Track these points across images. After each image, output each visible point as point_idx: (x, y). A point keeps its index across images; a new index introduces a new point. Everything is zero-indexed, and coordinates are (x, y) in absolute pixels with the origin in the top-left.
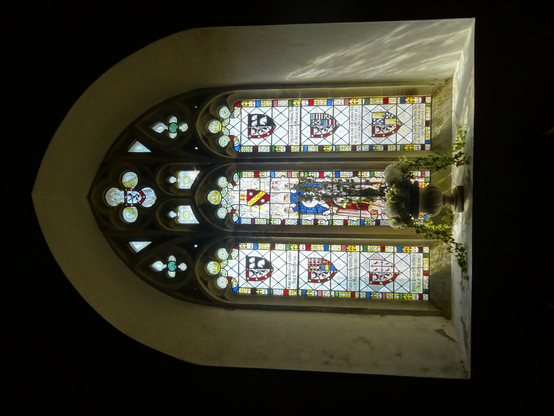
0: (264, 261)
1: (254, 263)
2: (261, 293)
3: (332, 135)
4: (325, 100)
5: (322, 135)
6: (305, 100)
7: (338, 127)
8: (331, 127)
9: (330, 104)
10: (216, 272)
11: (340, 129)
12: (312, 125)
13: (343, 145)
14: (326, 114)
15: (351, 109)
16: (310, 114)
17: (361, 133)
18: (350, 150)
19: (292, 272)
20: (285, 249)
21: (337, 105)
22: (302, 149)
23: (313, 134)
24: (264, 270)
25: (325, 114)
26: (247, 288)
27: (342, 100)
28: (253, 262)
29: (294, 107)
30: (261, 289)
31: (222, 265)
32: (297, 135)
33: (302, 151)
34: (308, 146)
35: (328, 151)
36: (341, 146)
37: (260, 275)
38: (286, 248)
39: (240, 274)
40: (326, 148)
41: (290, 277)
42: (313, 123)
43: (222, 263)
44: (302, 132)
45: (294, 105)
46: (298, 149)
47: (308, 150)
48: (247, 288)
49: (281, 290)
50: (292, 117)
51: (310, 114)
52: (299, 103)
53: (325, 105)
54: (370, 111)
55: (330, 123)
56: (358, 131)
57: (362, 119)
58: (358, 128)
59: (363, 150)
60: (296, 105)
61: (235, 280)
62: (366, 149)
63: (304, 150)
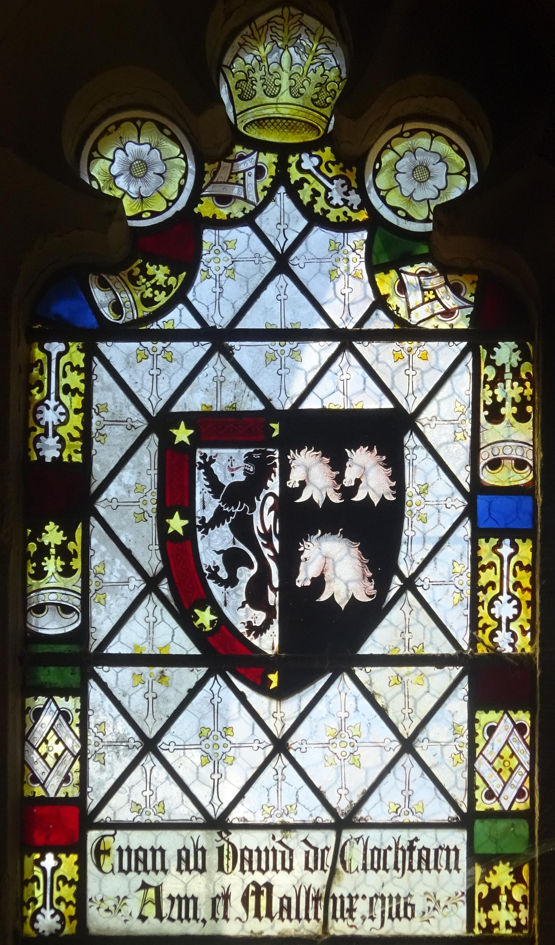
0: (362, 597)
1: (336, 499)
2: (40, 574)
10: (241, 105)
19: (261, 879)
20: (482, 805)
24: (273, 598)
26: (87, 422)
28: (348, 481)
30: (76, 564)
31: (309, 163)
37: (219, 560)
38: (490, 814)
39: (228, 354)
41: (212, 858)
43: (335, 170)
48: (87, 422)
49: (75, 777)
61: (162, 298)
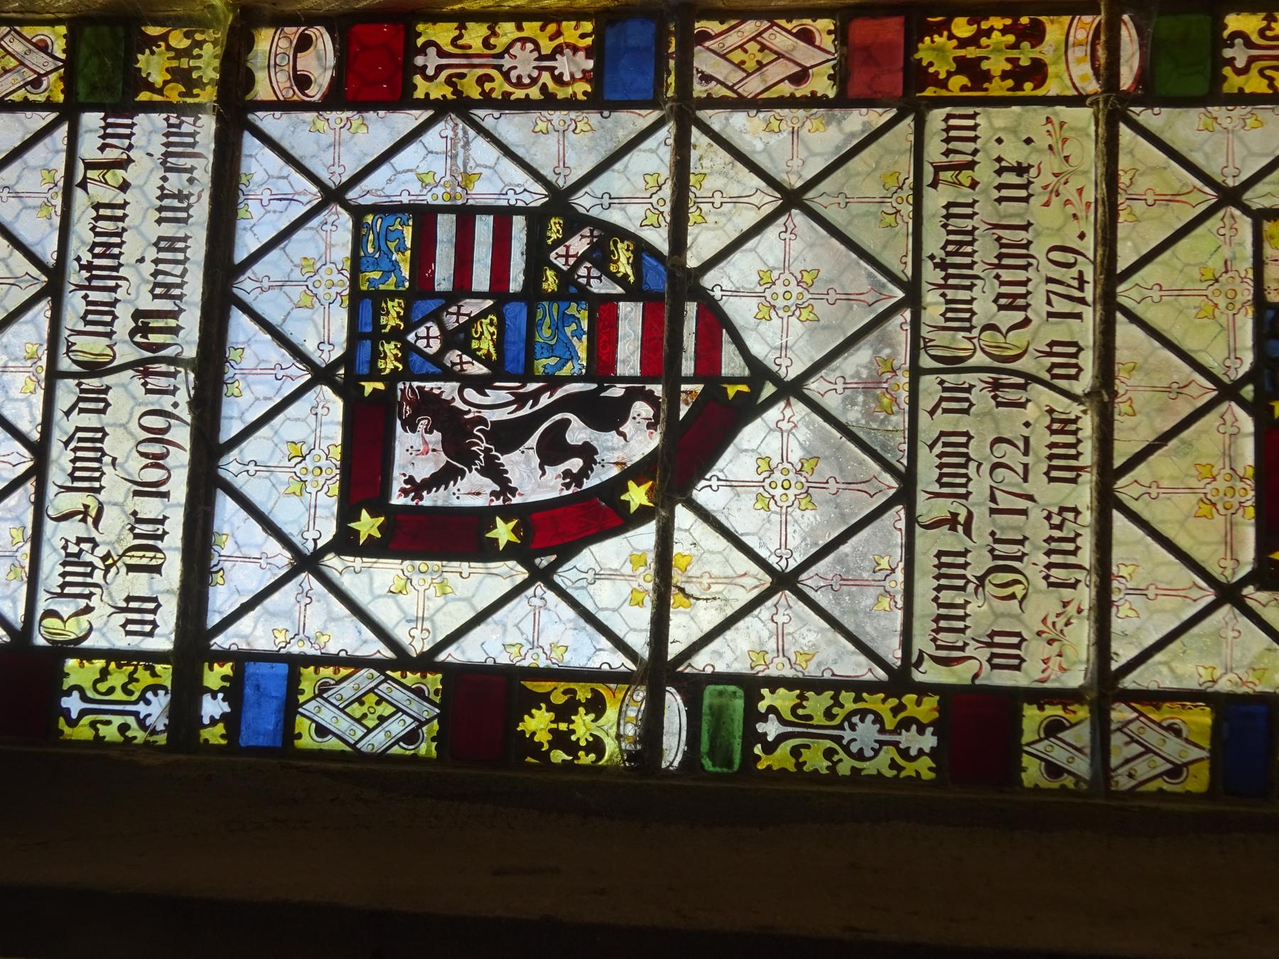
3: (645, 536)
4: (568, 26)
5: (507, 512)
6: (293, 32)
7: (748, 409)
8: (642, 409)
9: (647, 81)
11: (772, 447)
12: (375, 375)
13: (818, 685)
14: (575, 222)
15: (934, 150)
16: (358, 212)
17: (1087, 517)
18: (910, 769)
21: (740, 103)
22: (212, 707)
23: (379, 505)
25: (555, 229)
27: (806, 36)
29: (141, 119)
32: (149, 508)
33: (215, 735)
34: (296, 663)
35: (586, 759)
36: (783, 700)
40: (565, 712)
42: (390, 348)
44: (230, 467)
45: (144, 96)
46: (157, 709)
47: (289, 733)
50: (108, 247)
51: (358, 212)
52: (208, 64)
53: (562, 93)
54: (1230, 197)
55: (629, 357)
56: (1037, 485)
57: (1109, 306)
58: (1041, 440)
59: (1123, 783)
60: (174, 93)
62: (1176, 771)
63: (231, 721)
